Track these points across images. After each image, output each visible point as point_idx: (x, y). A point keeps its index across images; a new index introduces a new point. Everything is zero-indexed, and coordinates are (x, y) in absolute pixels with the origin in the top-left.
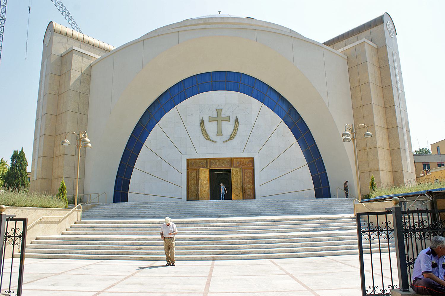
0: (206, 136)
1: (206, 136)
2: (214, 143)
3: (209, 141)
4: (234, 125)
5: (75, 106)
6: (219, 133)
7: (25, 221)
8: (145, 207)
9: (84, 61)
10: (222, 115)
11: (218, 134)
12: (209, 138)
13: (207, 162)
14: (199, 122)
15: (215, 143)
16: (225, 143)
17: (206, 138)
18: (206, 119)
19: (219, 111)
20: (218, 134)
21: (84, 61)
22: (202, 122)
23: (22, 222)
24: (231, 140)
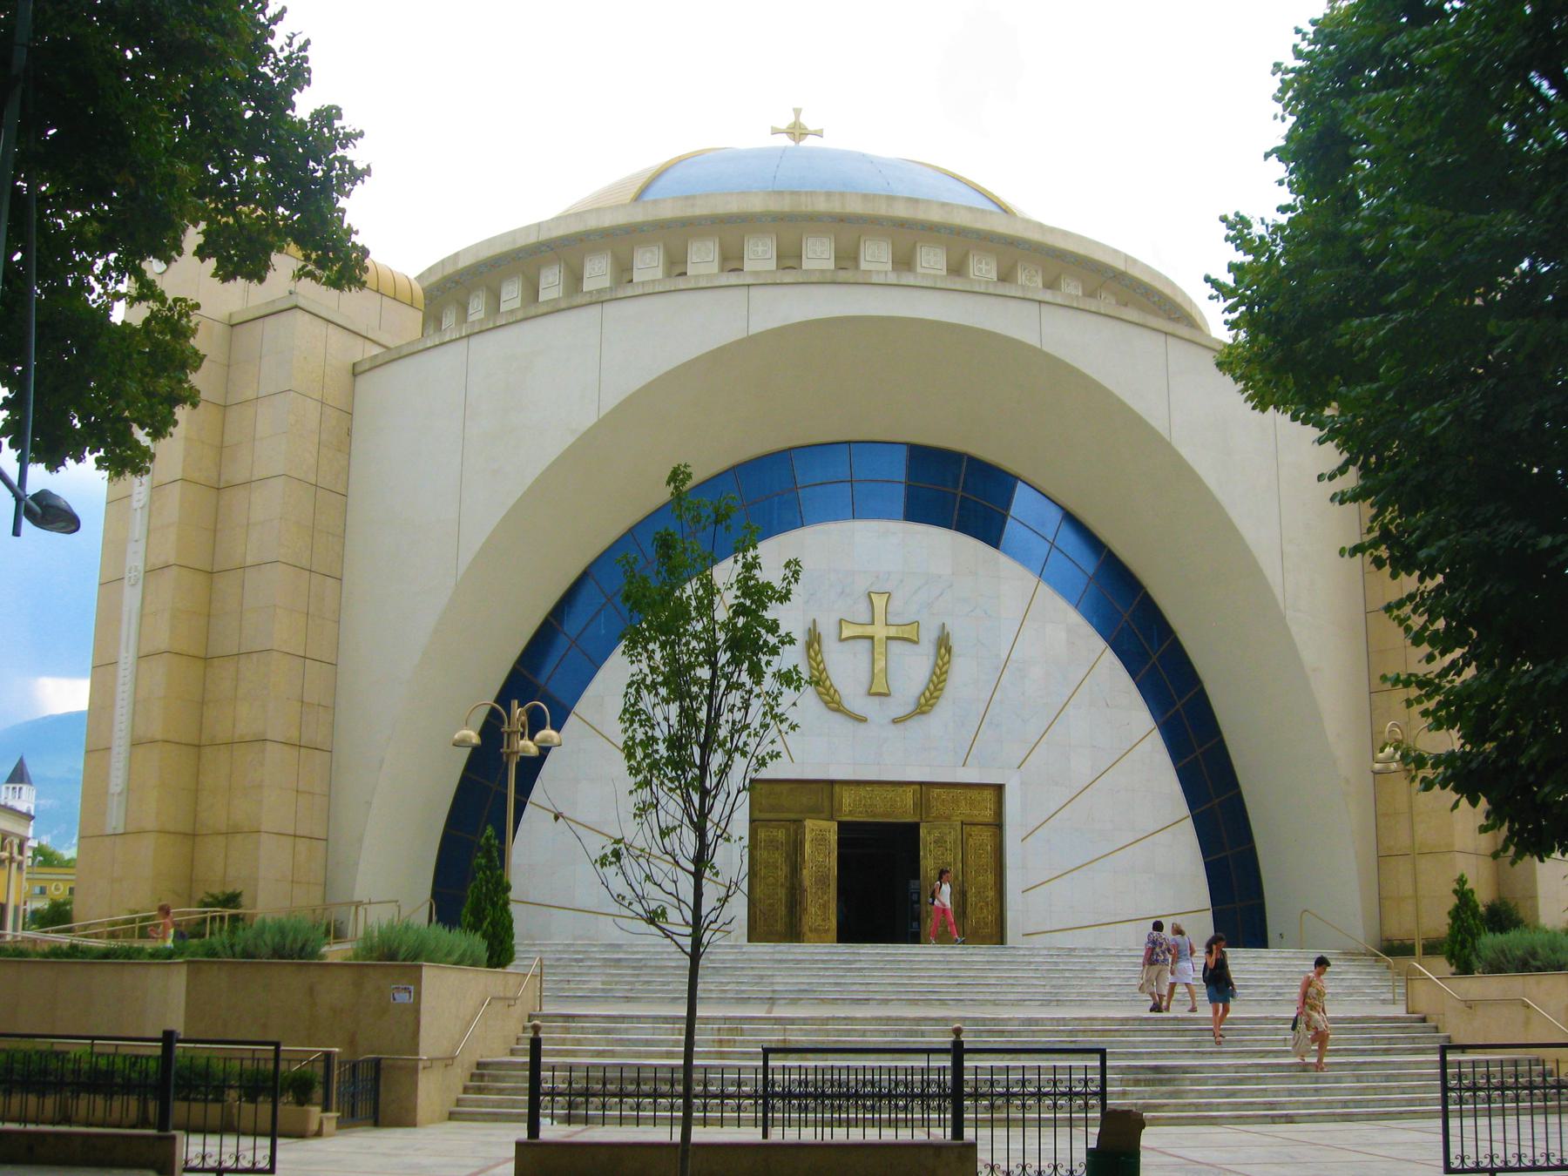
2: (856, 723)
3: (837, 716)
4: (932, 658)
7: (1102, 1053)
11: (872, 691)
12: (839, 703)
15: (862, 725)
16: (900, 726)
17: (826, 703)
18: (827, 629)
23: (1098, 1056)
24: (923, 717)
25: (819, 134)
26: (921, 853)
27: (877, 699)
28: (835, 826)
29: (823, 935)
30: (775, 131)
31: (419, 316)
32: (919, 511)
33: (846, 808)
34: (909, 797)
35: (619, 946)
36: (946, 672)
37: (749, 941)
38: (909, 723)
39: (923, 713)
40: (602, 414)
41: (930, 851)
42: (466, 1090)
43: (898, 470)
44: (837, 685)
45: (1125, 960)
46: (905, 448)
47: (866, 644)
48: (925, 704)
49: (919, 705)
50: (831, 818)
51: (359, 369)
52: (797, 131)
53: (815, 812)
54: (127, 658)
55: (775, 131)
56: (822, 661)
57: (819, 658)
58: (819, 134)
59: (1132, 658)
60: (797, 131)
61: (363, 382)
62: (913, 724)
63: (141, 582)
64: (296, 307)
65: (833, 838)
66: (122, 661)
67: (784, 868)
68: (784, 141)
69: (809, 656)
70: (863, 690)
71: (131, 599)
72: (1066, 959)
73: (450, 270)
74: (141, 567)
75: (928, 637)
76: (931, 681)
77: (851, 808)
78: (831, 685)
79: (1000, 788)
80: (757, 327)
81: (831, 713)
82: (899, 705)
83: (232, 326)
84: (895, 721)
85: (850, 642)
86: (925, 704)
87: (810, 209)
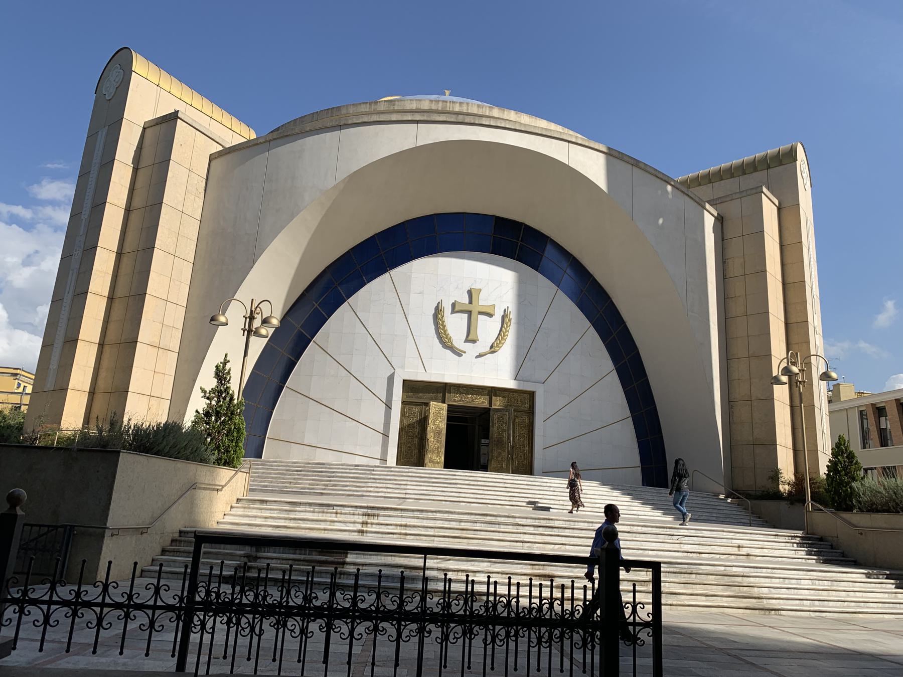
0: (446, 342)
1: (446, 342)
5: (169, 239)
6: (470, 339)
9: (197, 147)
13: (441, 390)
20: (470, 338)
21: (197, 147)
26: (491, 424)
28: (445, 406)
29: (436, 465)
35: (323, 464)
37: (397, 465)
41: (495, 423)
42: (164, 552)
44: (451, 335)
47: (466, 316)
50: (444, 402)
51: (212, 157)
53: (436, 400)
59: (604, 335)
65: (445, 413)
67: (418, 427)
82: (483, 344)
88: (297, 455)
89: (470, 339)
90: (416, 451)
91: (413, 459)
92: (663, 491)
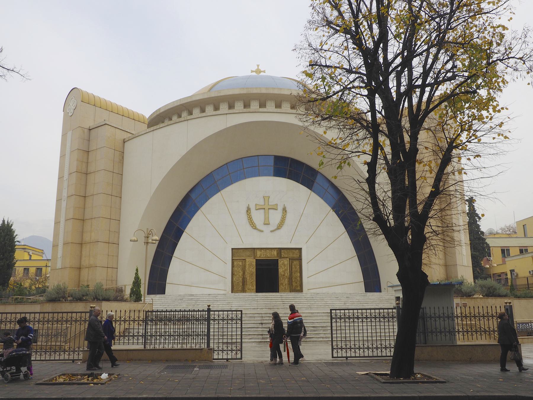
2: (260, 232)
3: (255, 231)
8: (192, 299)
10: (269, 203)
14: (245, 209)
19: (266, 198)
22: (248, 210)
24: (279, 230)
25: (264, 72)
27: (266, 225)
28: (255, 260)
30: (252, 72)
31: (147, 125)
32: (278, 173)
33: (258, 256)
34: (275, 253)
35: (193, 295)
36: (285, 217)
38: (275, 232)
39: (279, 229)
40: (188, 151)
43: (271, 162)
45: (333, 296)
46: (273, 156)
47: (262, 211)
48: (280, 226)
49: (278, 227)
51: (125, 141)
52: (258, 71)
54: (62, 220)
55: (252, 72)
56: (251, 215)
57: (250, 215)
58: (264, 72)
60: (258, 71)
61: (126, 144)
62: (278, 232)
63: (66, 200)
64: (106, 124)
65: (254, 264)
66: (61, 221)
68: (254, 74)
69: (247, 214)
70: (262, 223)
71: (64, 204)
72: (316, 296)
73: (158, 113)
74: (66, 196)
75: (280, 208)
76: (281, 220)
77: (260, 255)
78: (253, 222)
79: (300, 249)
80: (228, 126)
81: (254, 230)
82: (273, 227)
83: (90, 130)
84: (271, 231)
85: (259, 210)
86: (280, 226)
87: (251, 92)
88: (183, 291)
89: (267, 224)
90: (241, 284)
91: (240, 289)
92: (369, 294)
